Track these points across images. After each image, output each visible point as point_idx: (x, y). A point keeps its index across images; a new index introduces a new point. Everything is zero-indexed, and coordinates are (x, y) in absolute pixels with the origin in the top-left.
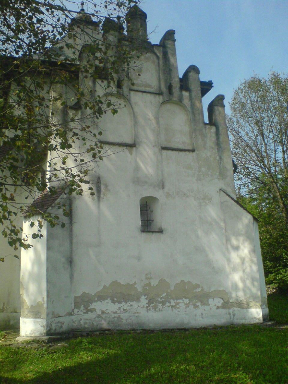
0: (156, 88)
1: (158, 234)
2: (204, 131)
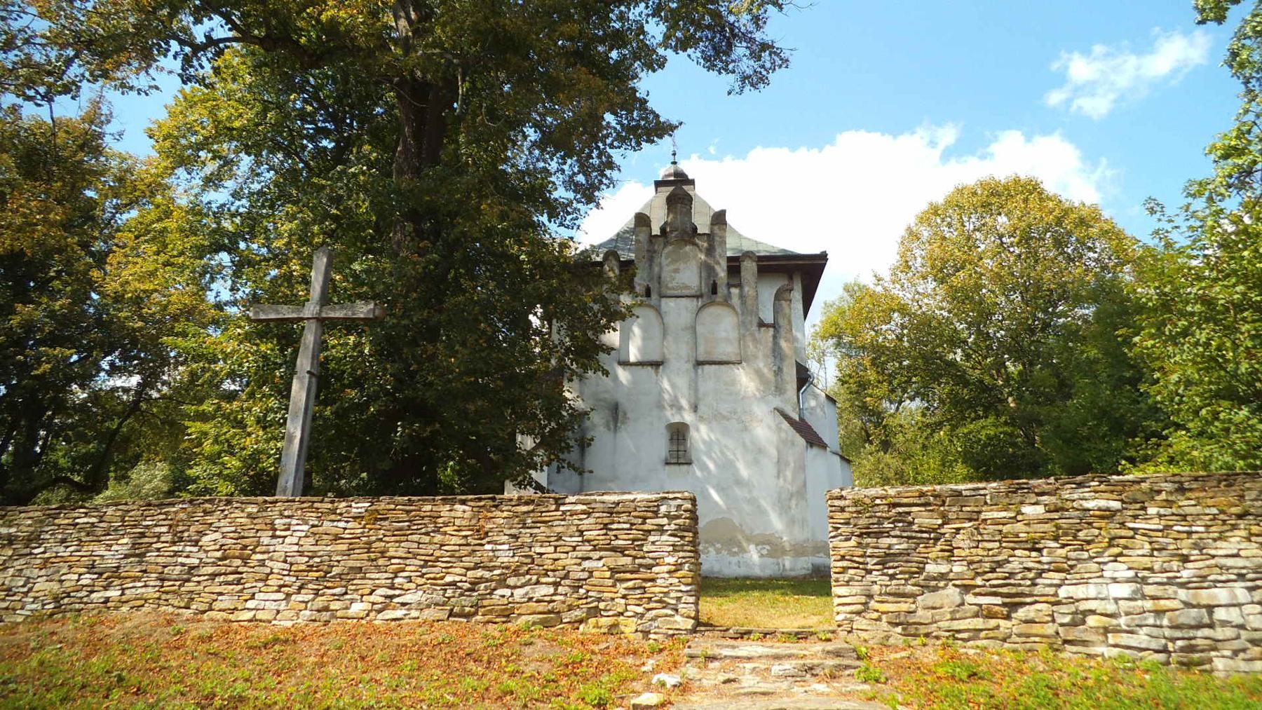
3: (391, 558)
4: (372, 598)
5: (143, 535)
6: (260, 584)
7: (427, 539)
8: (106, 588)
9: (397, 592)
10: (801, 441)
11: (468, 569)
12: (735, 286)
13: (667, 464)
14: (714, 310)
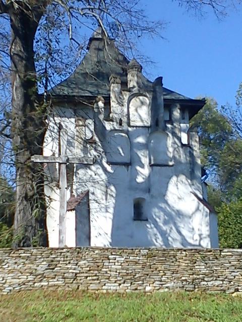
5: (52, 261)
6: (107, 280)
7: (173, 264)
8: (41, 281)
9: (164, 283)
11: (190, 275)
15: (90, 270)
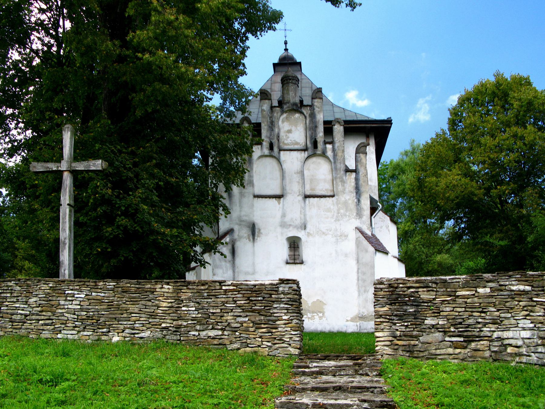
0: (303, 144)
1: (299, 265)
2: (344, 178)
3: (132, 313)
4: (124, 334)
6: (63, 326)
7: (150, 303)
9: (137, 332)
10: (372, 249)
12: (330, 143)
13: (287, 263)
14: (314, 159)
15: (42, 311)
